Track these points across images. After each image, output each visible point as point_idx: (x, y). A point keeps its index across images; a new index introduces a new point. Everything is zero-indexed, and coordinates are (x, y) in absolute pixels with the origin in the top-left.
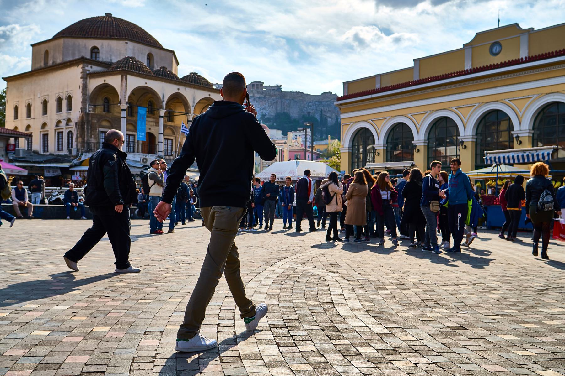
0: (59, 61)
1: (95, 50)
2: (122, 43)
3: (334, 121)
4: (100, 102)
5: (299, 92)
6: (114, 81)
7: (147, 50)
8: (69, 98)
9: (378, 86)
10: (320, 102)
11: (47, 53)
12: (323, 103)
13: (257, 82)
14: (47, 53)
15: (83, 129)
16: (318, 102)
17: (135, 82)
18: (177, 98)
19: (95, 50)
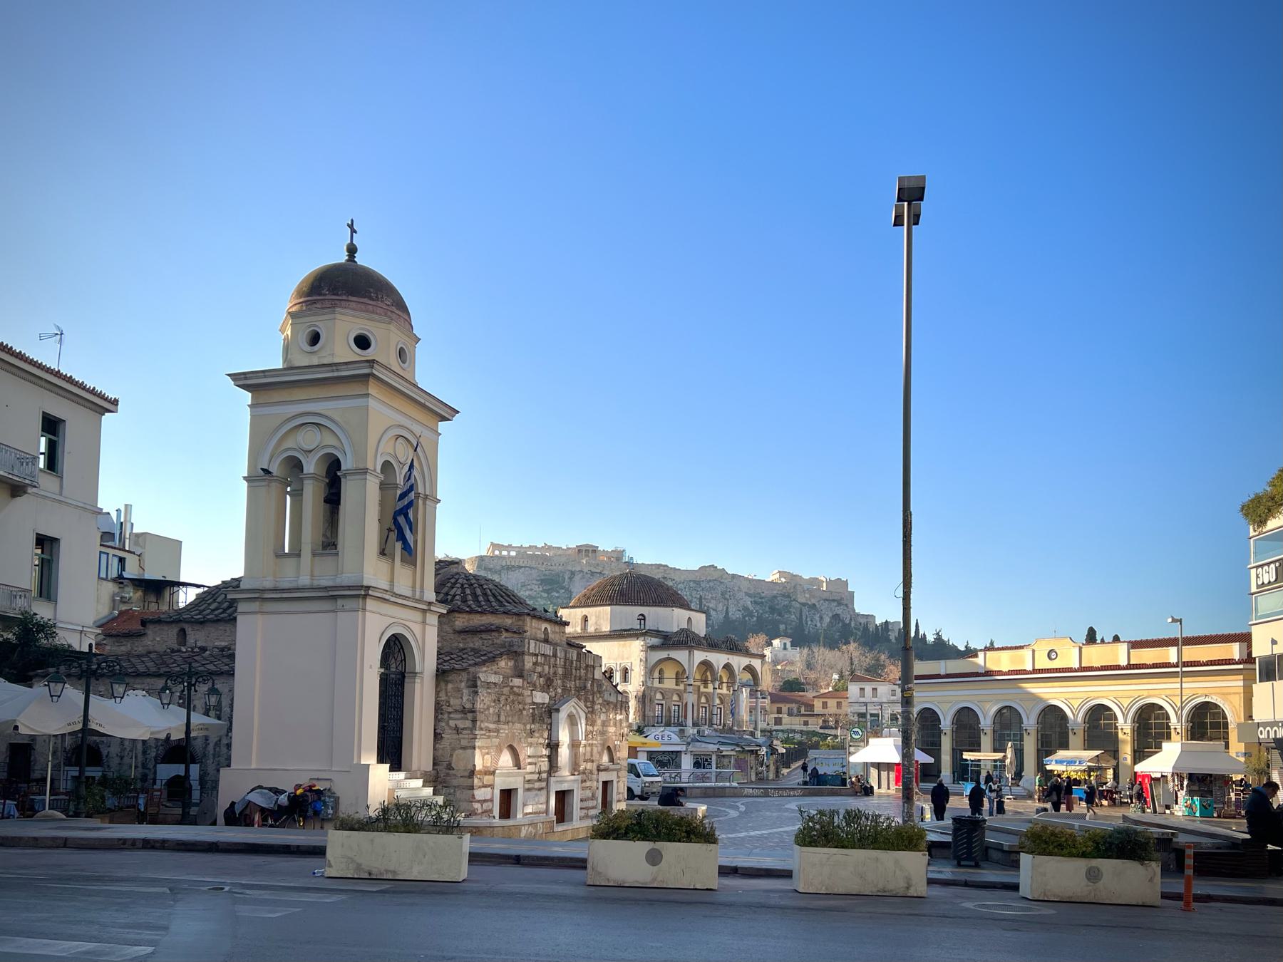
0: (606, 628)
1: (642, 618)
2: (668, 610)
3: (722, 616)
4: (656, 675)
5: (660, 565)
6: (681, 655)
7: (686, 614)
8: (625, 672)
9: (943, 672)
10: (697, 583)
11: (585, 619)
12: (703, 585)
13: (587, 545)
14: (585, 619)
15: (644, 702)
16: (694, 582)
17: (699, 656)
18: (728, 667)
19: (642, 618)
